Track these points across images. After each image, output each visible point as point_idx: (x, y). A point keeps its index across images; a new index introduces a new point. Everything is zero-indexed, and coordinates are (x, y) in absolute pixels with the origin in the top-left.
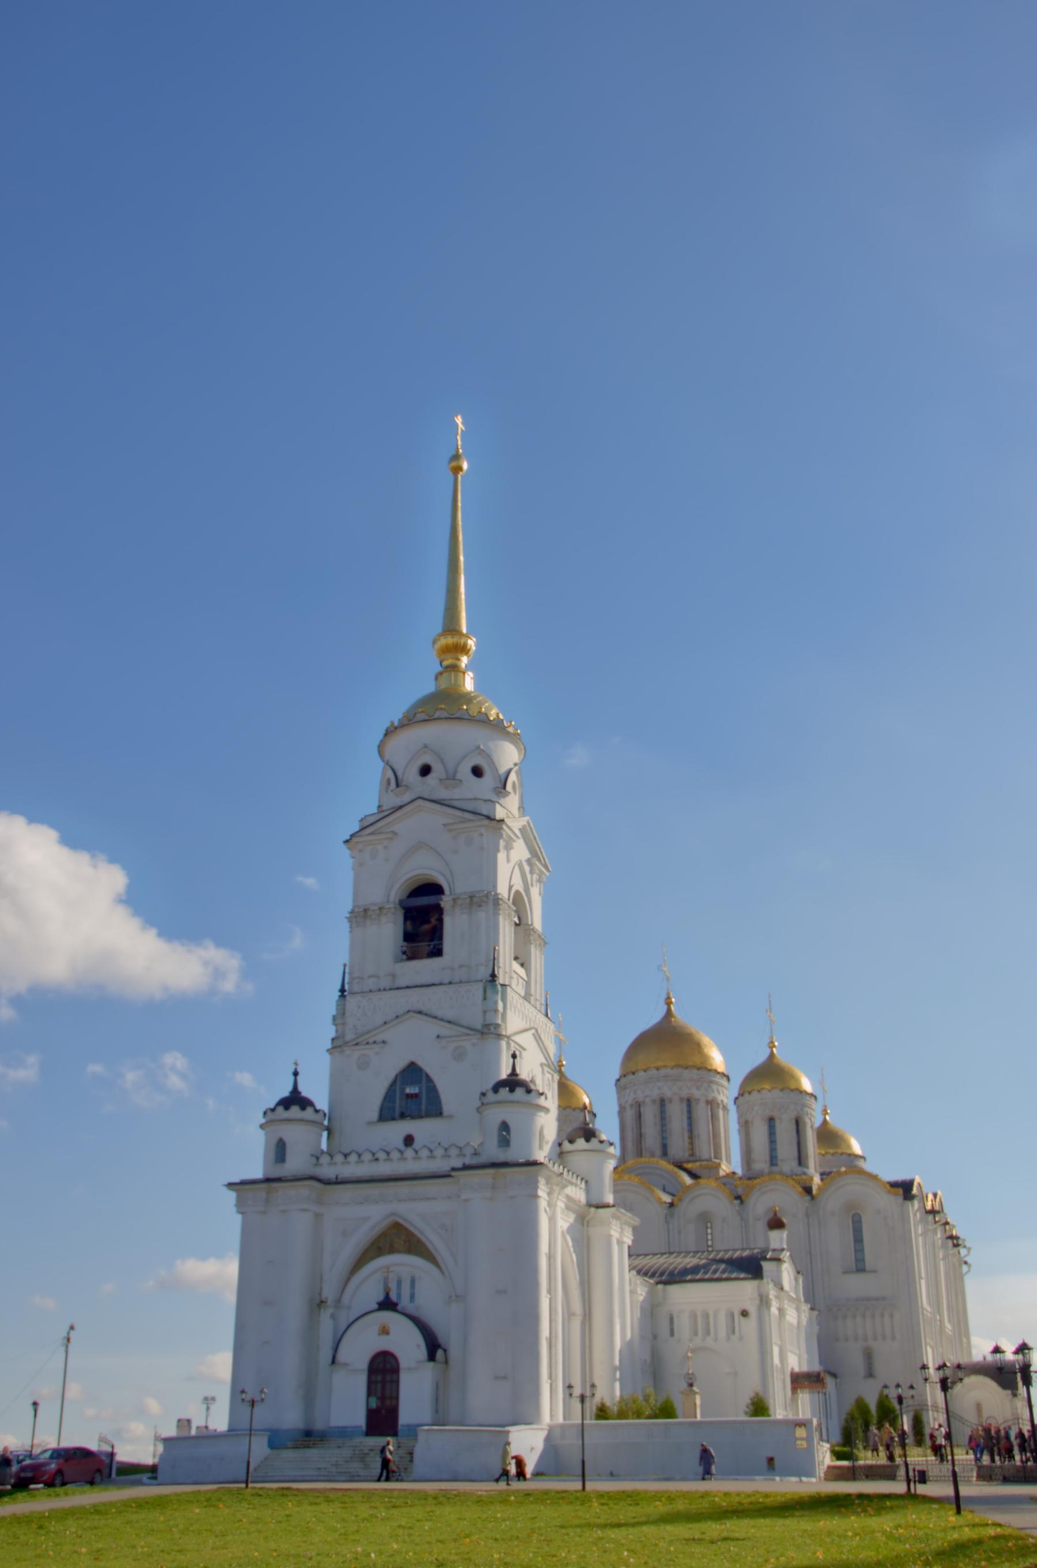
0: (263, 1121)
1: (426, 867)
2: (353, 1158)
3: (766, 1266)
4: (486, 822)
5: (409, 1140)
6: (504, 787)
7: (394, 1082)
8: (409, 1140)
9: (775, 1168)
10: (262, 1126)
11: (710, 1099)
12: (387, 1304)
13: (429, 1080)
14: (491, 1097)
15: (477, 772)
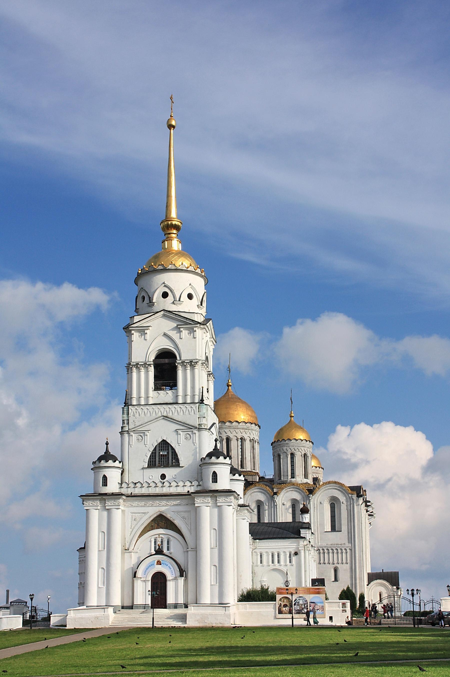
0: (93, 466)
1: (167, 345)
2: (139, 485)
3: (302, 531)
4: (198, 325)
5: (163, 477)
6: (201, 305)
7: (155, 449)
8: (163, 477)
9: (292, 479)
10: (92, 469)
11: (251, 439)
12: (159, 552)
13: (173, 449)
14: (207, 460)
15: (190, 296)
